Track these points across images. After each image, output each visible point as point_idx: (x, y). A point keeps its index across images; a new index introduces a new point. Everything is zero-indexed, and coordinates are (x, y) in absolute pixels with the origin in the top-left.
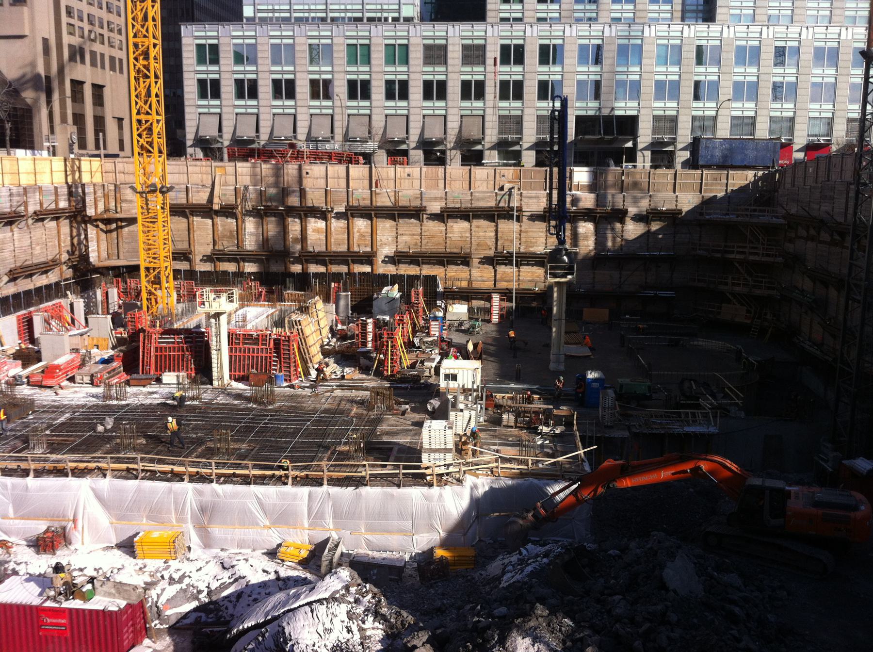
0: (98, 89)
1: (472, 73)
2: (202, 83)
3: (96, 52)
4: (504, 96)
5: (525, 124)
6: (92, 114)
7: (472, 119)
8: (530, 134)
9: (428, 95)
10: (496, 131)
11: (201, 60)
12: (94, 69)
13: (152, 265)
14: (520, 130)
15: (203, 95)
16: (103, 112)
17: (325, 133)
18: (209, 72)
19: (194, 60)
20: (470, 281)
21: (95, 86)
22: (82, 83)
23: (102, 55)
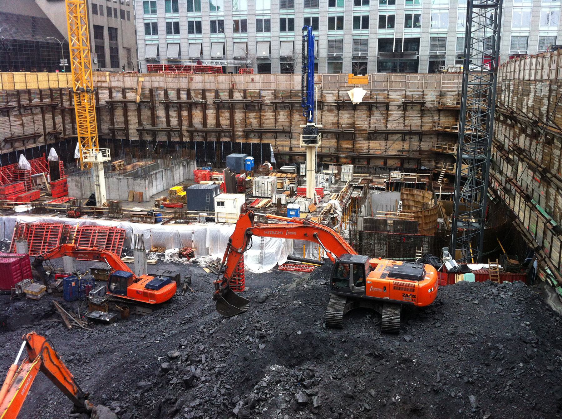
0: (113, 32)
1: (312, 13)
2: (147, 25)
3: (111, 8)
4: (331, 27)
5: (345, 45)
6: (109, 46)
7: (263, 44)
8: (348, 53)
9: (283, 29)
10: (326, 50)
11: (146, 11)
12: (109, 18)
13: (84, 136)
14: (341, 50)
15: (147, 33)
16: (117, 44)
17: (219, 54)
18: (150, 18)
19: (142, 12)
20: (291, 148)
21: (110, 29)
22: (101, 28)
23: (115, 10)
